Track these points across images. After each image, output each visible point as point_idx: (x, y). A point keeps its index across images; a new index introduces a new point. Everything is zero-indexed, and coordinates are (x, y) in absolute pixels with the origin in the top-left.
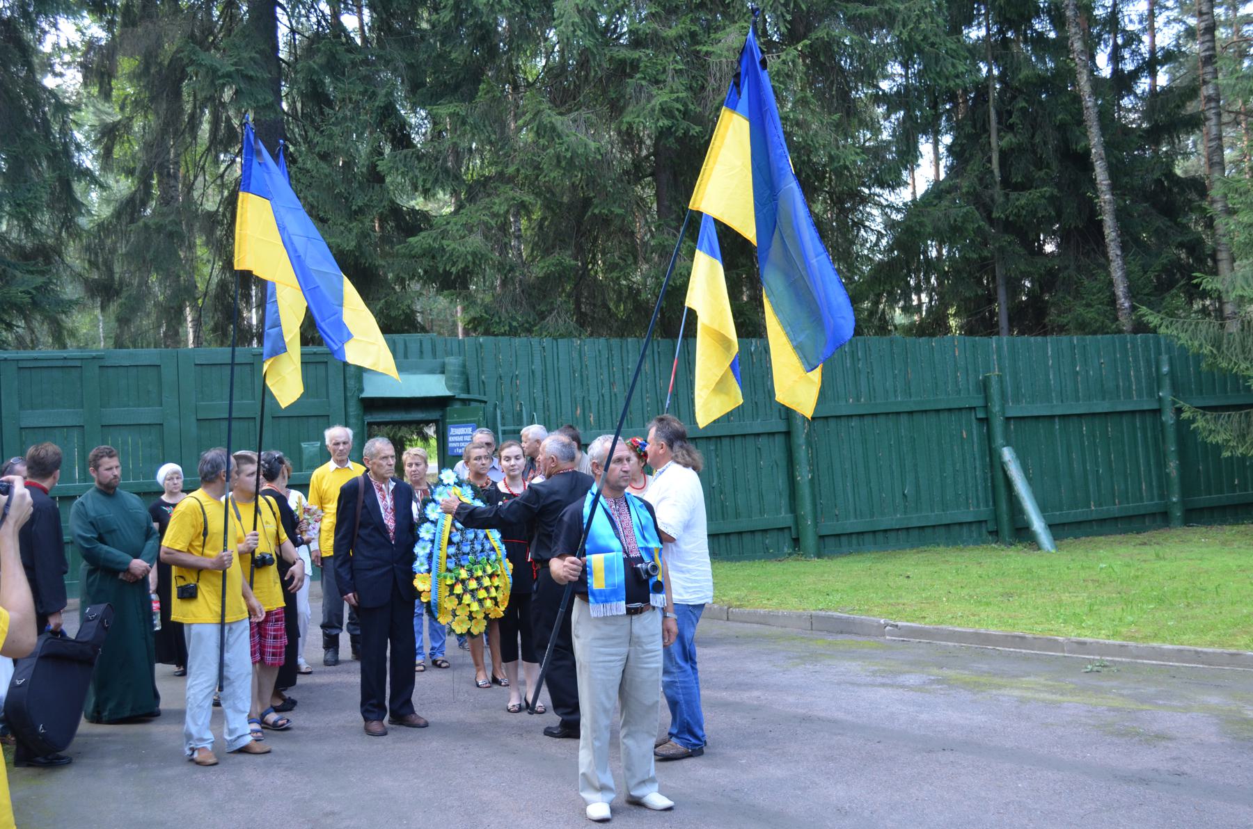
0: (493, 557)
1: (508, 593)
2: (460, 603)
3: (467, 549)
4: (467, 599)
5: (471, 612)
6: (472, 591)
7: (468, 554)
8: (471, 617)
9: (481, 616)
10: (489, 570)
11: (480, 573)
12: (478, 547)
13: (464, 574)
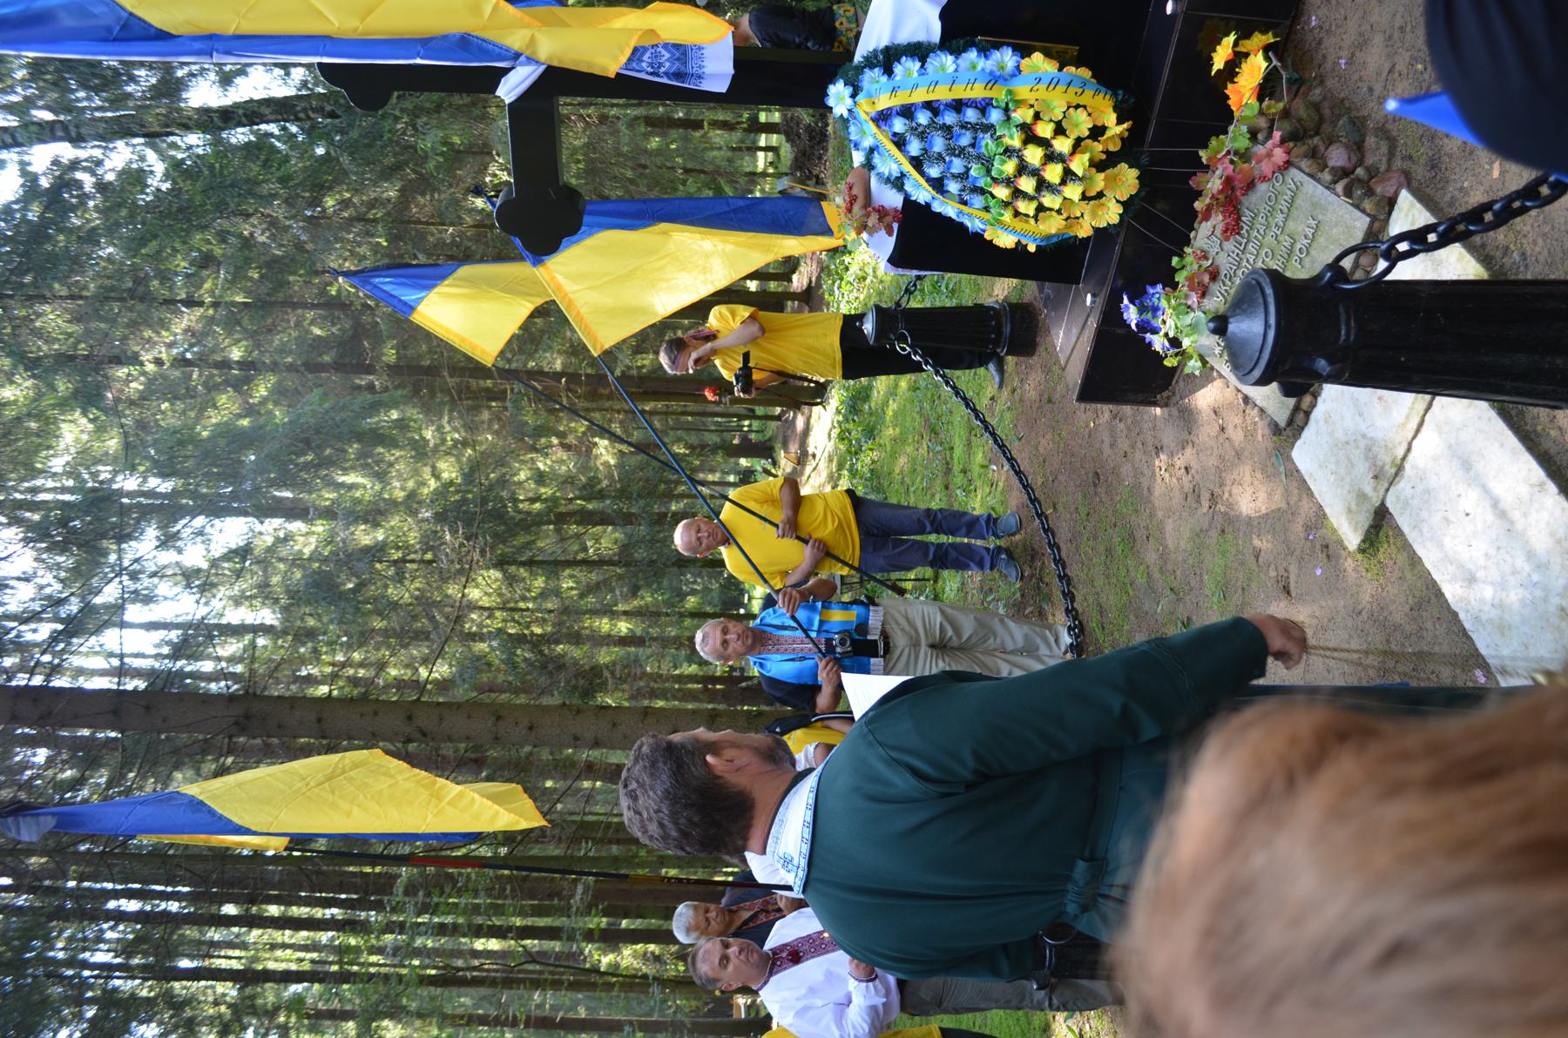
4: (1048, 200)
5: (1084, 197)
7: (968, 169)
9: (1099, 181)
11: (1010, 167)
12: (965, 141)
13: (1002, 193)
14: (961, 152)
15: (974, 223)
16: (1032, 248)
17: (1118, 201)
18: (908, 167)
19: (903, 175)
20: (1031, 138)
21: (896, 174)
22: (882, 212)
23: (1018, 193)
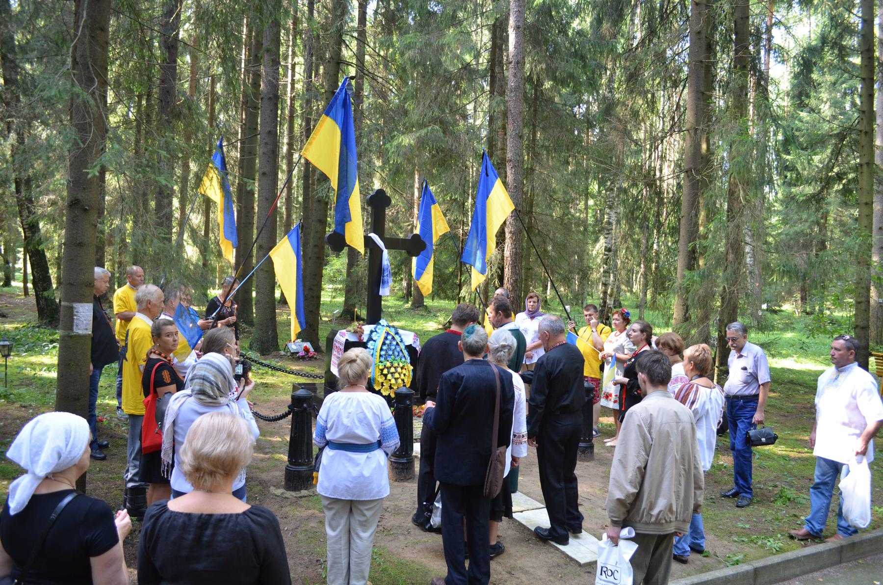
0: (403, 359)
1: (410, 380)
2: (386, 379)
3: (390, 353)
6: (392, 373)
8: (391, 388)
10: (401, 365)
11: (396, 365)
12: (396, 353)
14: (393, 353)
19: (375, 341)
20: (402, 368)
21: (374, 339)
23: (389, 368)
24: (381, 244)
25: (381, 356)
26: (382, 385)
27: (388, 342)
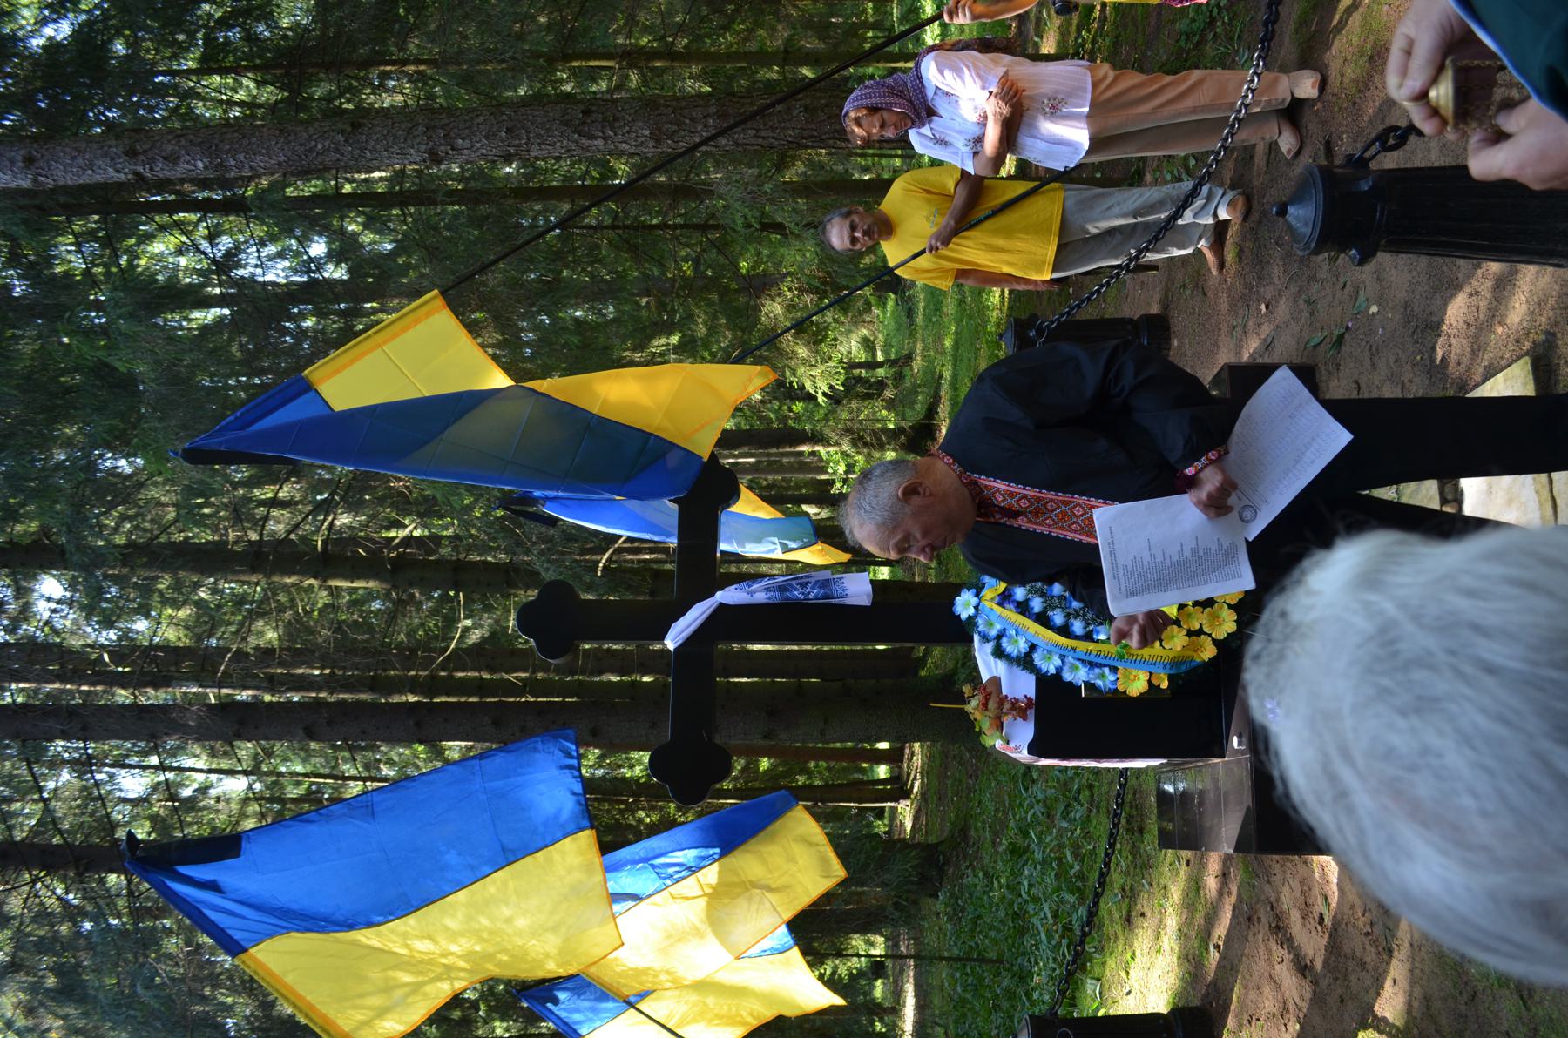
2: (1177, 622)
15: (1105, 680)
16: (1165, 685)
17: (1230, 606)
18: (1034, 628)
19: (1033, 647)
21: (1022, 646)
22: (1015, 702)
24: (696, 614)
25: (1088, 637)
26: (1200, 632)
27: (1037, 604)
